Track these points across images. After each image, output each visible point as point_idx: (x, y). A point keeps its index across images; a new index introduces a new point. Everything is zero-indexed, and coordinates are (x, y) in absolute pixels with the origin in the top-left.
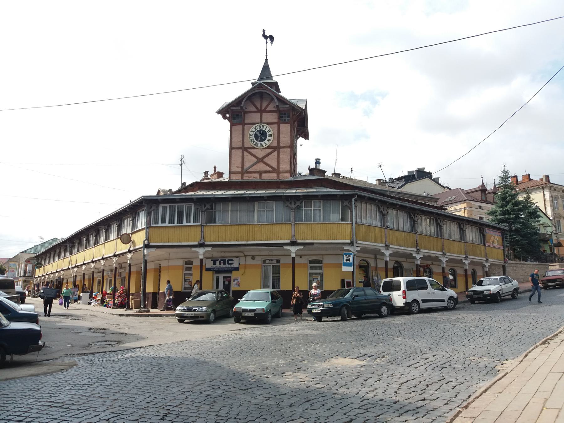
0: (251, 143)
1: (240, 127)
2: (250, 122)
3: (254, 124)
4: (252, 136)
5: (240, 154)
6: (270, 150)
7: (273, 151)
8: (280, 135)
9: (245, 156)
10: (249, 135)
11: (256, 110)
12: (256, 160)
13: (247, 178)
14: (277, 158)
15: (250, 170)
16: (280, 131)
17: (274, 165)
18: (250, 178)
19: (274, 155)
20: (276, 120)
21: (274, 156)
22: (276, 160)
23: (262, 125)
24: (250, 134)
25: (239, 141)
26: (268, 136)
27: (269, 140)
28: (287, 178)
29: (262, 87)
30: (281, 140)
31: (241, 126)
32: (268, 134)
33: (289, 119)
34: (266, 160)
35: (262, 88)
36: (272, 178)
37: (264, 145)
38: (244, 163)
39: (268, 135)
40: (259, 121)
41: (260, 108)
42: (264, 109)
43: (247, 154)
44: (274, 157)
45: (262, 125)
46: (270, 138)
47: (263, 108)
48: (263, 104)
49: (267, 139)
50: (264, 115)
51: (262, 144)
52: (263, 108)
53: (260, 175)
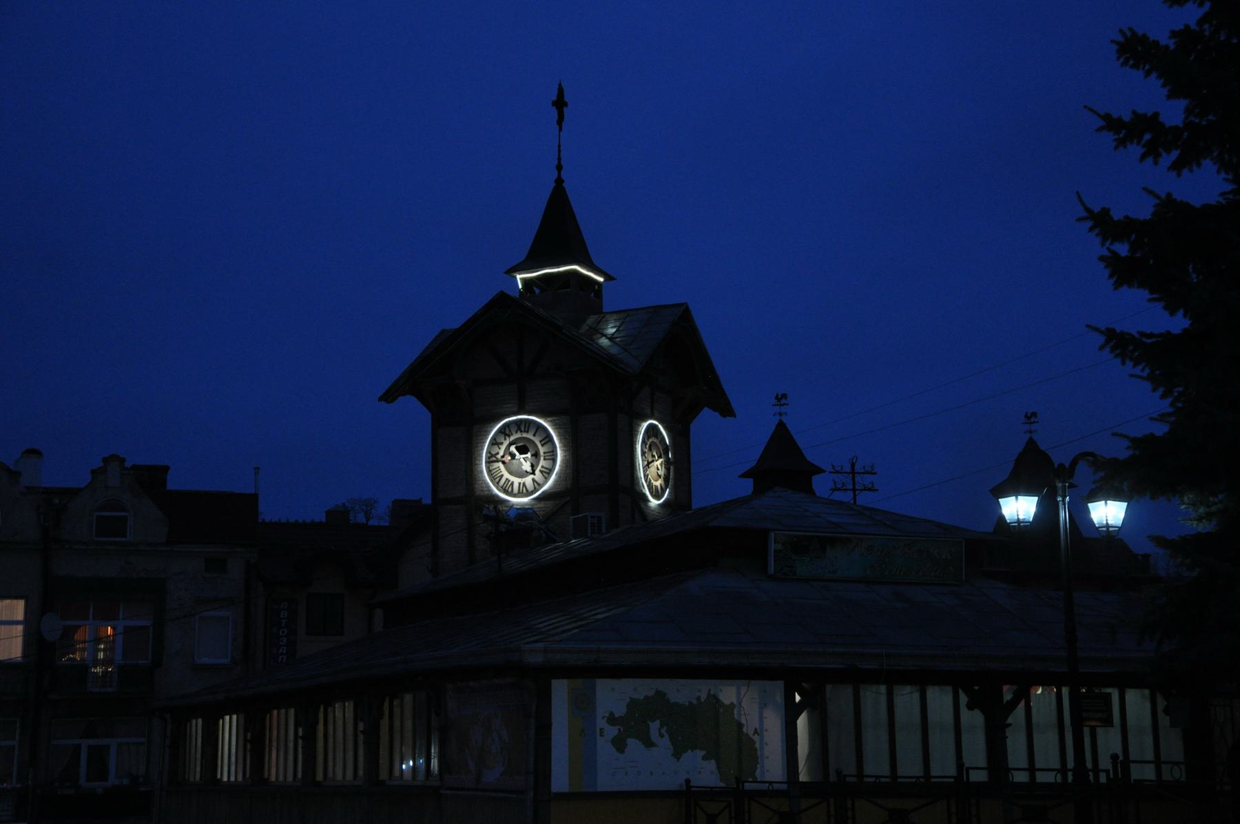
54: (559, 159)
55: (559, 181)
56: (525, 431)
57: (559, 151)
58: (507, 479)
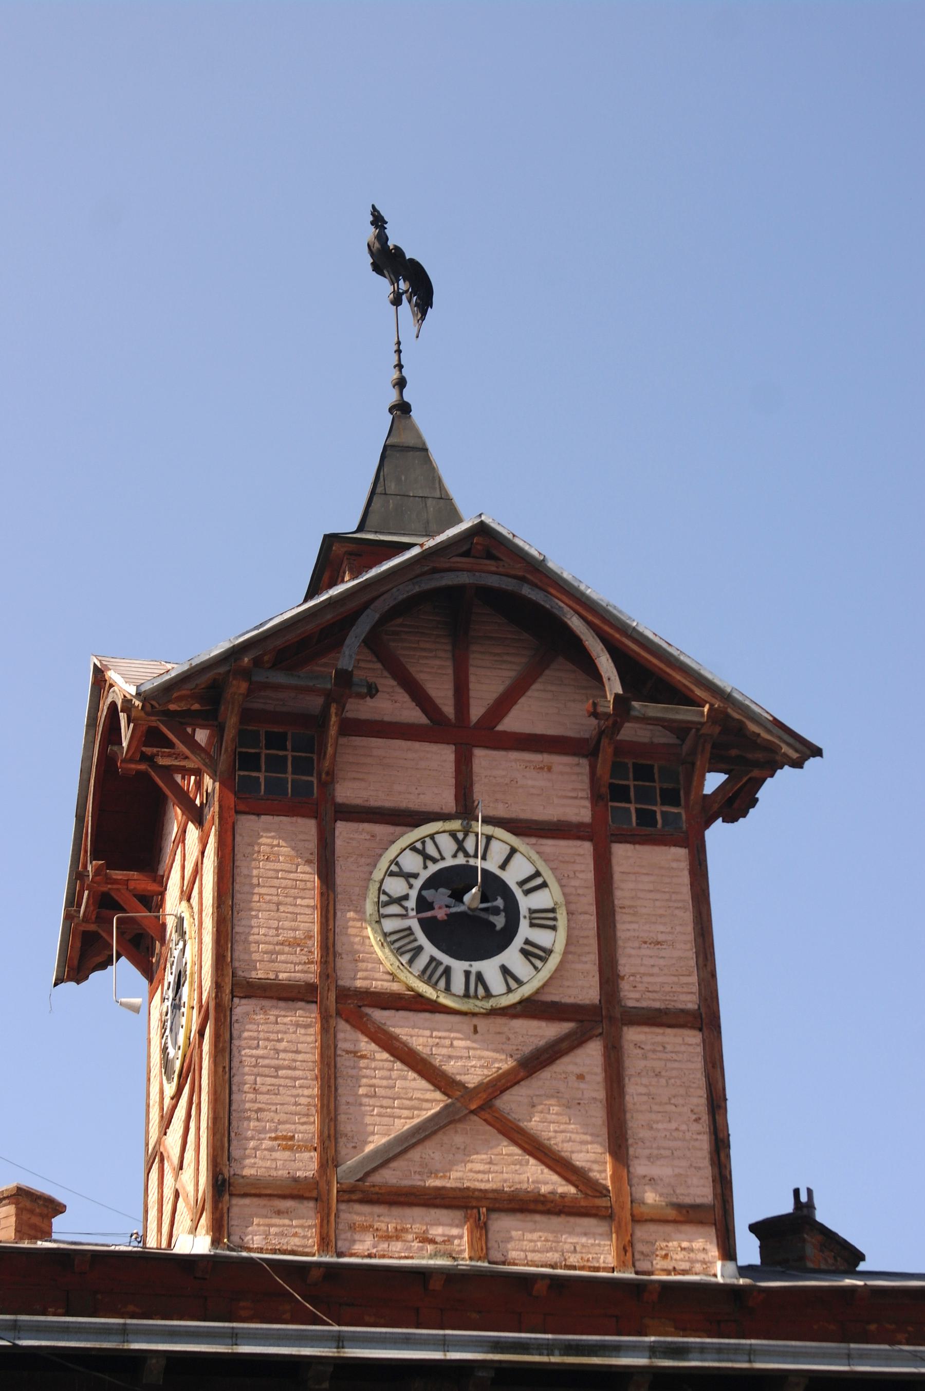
2: (373, 803)
3: (414, 819)
4: (394, 909)
8: (619, 926)
12: (438, 1095)
14: (601, 1095)
15: (390, 1177)
16: (618, 894)
18: (397, 1246)
19: (577, 1070)
21: (581, 1077)
24: (381, 891)
26: (524, 924)
27: (532, 953)
29: (490, 556)
30: (626, 966)
31: (308, 827)
32: (525, 903)
35: (491, 565)
36: (573, 1260)
37: (496, 983)
38: (342, 1118)
39: (523, 911)
40: (446, 799)
41: (449, 709)
42: (483, 717)
43: (366, 1045)
44: (582, 1086)
46: (543, 937)
47: (476, 712)
48: (472, 678)
49: (518, 942)
50: (482, 758)
51: (480, 977)
52: (476, 712)
55: (402, 409)
57: (399, 351)
58: (432, 959)
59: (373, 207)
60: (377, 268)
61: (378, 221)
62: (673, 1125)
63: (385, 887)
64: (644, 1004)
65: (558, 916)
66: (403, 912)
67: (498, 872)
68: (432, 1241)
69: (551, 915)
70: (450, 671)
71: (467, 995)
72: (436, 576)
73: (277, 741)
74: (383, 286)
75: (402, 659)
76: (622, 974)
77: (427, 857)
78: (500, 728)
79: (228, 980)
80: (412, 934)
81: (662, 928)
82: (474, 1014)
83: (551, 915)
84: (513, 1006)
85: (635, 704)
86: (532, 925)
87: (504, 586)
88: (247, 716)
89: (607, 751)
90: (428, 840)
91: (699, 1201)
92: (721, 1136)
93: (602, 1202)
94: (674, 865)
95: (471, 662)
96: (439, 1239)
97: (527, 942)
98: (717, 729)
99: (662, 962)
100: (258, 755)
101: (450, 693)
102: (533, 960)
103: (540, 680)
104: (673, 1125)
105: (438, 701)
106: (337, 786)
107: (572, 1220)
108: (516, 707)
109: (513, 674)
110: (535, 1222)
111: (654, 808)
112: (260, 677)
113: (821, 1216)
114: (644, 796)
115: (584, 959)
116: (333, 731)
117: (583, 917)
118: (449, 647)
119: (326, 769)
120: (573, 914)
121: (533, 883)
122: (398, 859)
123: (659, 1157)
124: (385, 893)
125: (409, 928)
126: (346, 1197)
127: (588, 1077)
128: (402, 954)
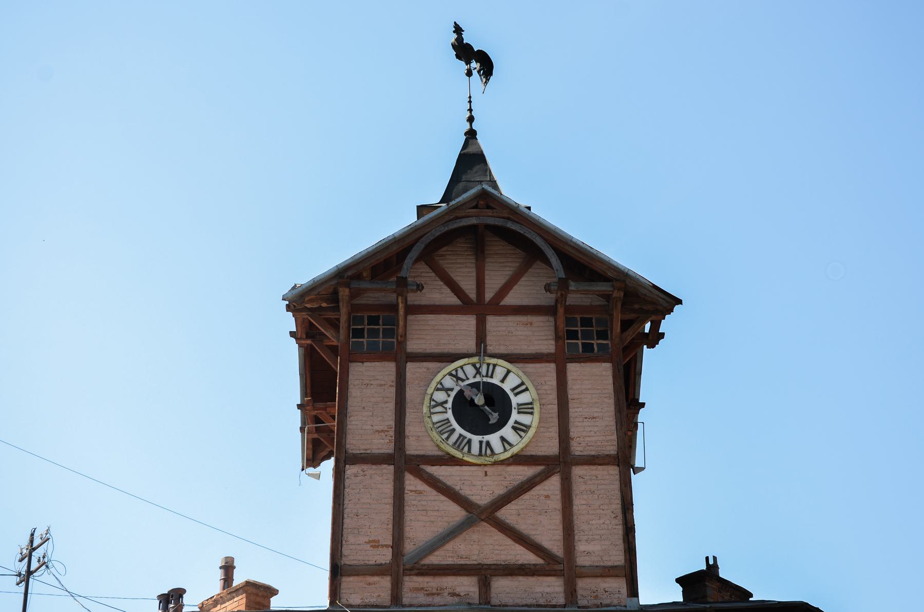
0: (434, 434)
1: (385, 371)
2: (428, 351)
4: (439, 409)
5: (388, 488)
6: (525, 472)
7: (539, 474)
8: (571, 410)
9: (409, 497)
10: (427, 398)
11: (458, 302)
13: (422, 599)
14: (559, 505)
15: (435, 559)
17: (551, 540)
19: (545, 493)
20: (548, 346)
22: (557, 519)
23: (488, 365)
24: (431, 399)
25: (380, 428)
27: (519, 428)
28: (615, 602)
29: (488, 207)
30: (574, 432)
31: (389, 368)
32: (515, 400)
33: (605, 342)
34: (507, 514)
35: (489, 212)
36: (542, 602)
37: (497, 446)
38: (407, 529)
39: (514, 405)
40: (470, 344)
41: (473, 295)
44: (548, 502)
45: (488, 365)
46: (525, 419)
47: (489, 295)
48: (486, 277)
49: (511, 422)
50: (493, 323)
51: (488, 444)
52: (489, 295)
53: (485, 586)
54: (470, 110)
55: (471, 134)
56: (487, 376)
57: (470, 102)
58: (461, 435)
59: (455, 23)
60: (458, 57)
61: (458, 30)
62: (602, 521)
63: (434, 397)
64: (585, 453)
65: (535, 407)
66: (445, 411)
67: (499, 384)
68: (459, 595)
69: (530, 406)
70: (474, 274)
71: (480, 454)
72: (458, 221)
73: (373, 321)
74: (462, 66)
75: (446, 270)
76: (572, 437)
77: (458, 379)
78: (502, 303)
79: (343, 455)
80: (449, 422)
81: (596, 410)
82: (485, 465)
83: (530, 406)
84: (508, 459)
85: (572, 283)
86: (519, 413)
87: (496, 223)
88: (354, 308)
89: (561, 311)
90: (459, 370)
91: (616, 564)
92: (629, 525)
93: (560, 567)
94: (604, 373)
95: (486, 268)
96: (462, 594)
97: (516, 422)
98: (622, 294)
99: (596, 429)
100: (363, 329)
101: (474, 287)
102: (519, 432)
103: (526, 275)
104: (602, 521)
105: (467, 292)
106: (408, 343)
107: (541, 578)
108: (512, 291)
109: (510, 273)
110: (519, 581)
111: (592, 342)
112: (355, 285)
113: (722, 574)
114: (586, 335)
115: (550, 430)
116: (401, 312)
117: (550, 406)
118: (474, 261)
119: (400, 334)
120: (544, 405)
121: (519, 389)
122: (442, 381)
123: (593, 540)
124: (434, 400)
125: (448, 419)
126: (408, 572)
127: (552, 497)
128: (442, 434)
